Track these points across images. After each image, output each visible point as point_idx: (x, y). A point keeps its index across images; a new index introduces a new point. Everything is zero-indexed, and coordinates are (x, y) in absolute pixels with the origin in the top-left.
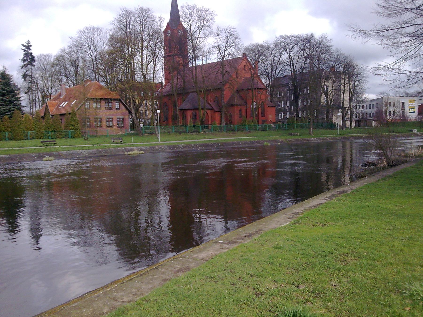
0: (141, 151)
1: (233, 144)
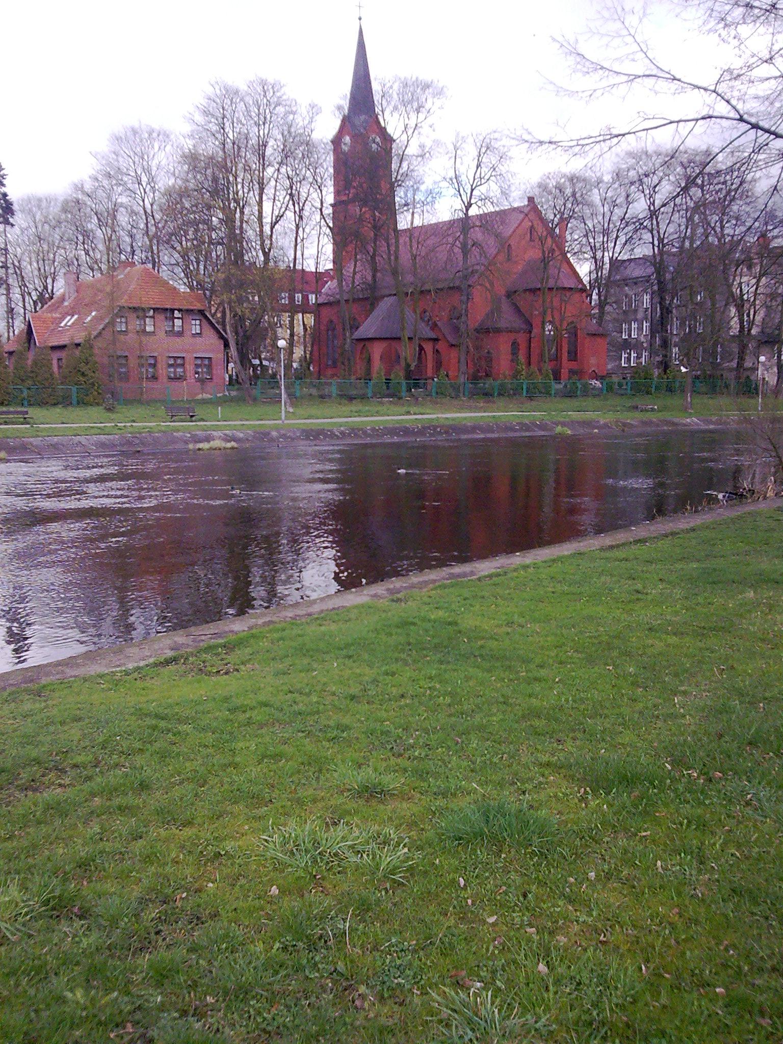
0: (229, 441)
1: (474, 429)
